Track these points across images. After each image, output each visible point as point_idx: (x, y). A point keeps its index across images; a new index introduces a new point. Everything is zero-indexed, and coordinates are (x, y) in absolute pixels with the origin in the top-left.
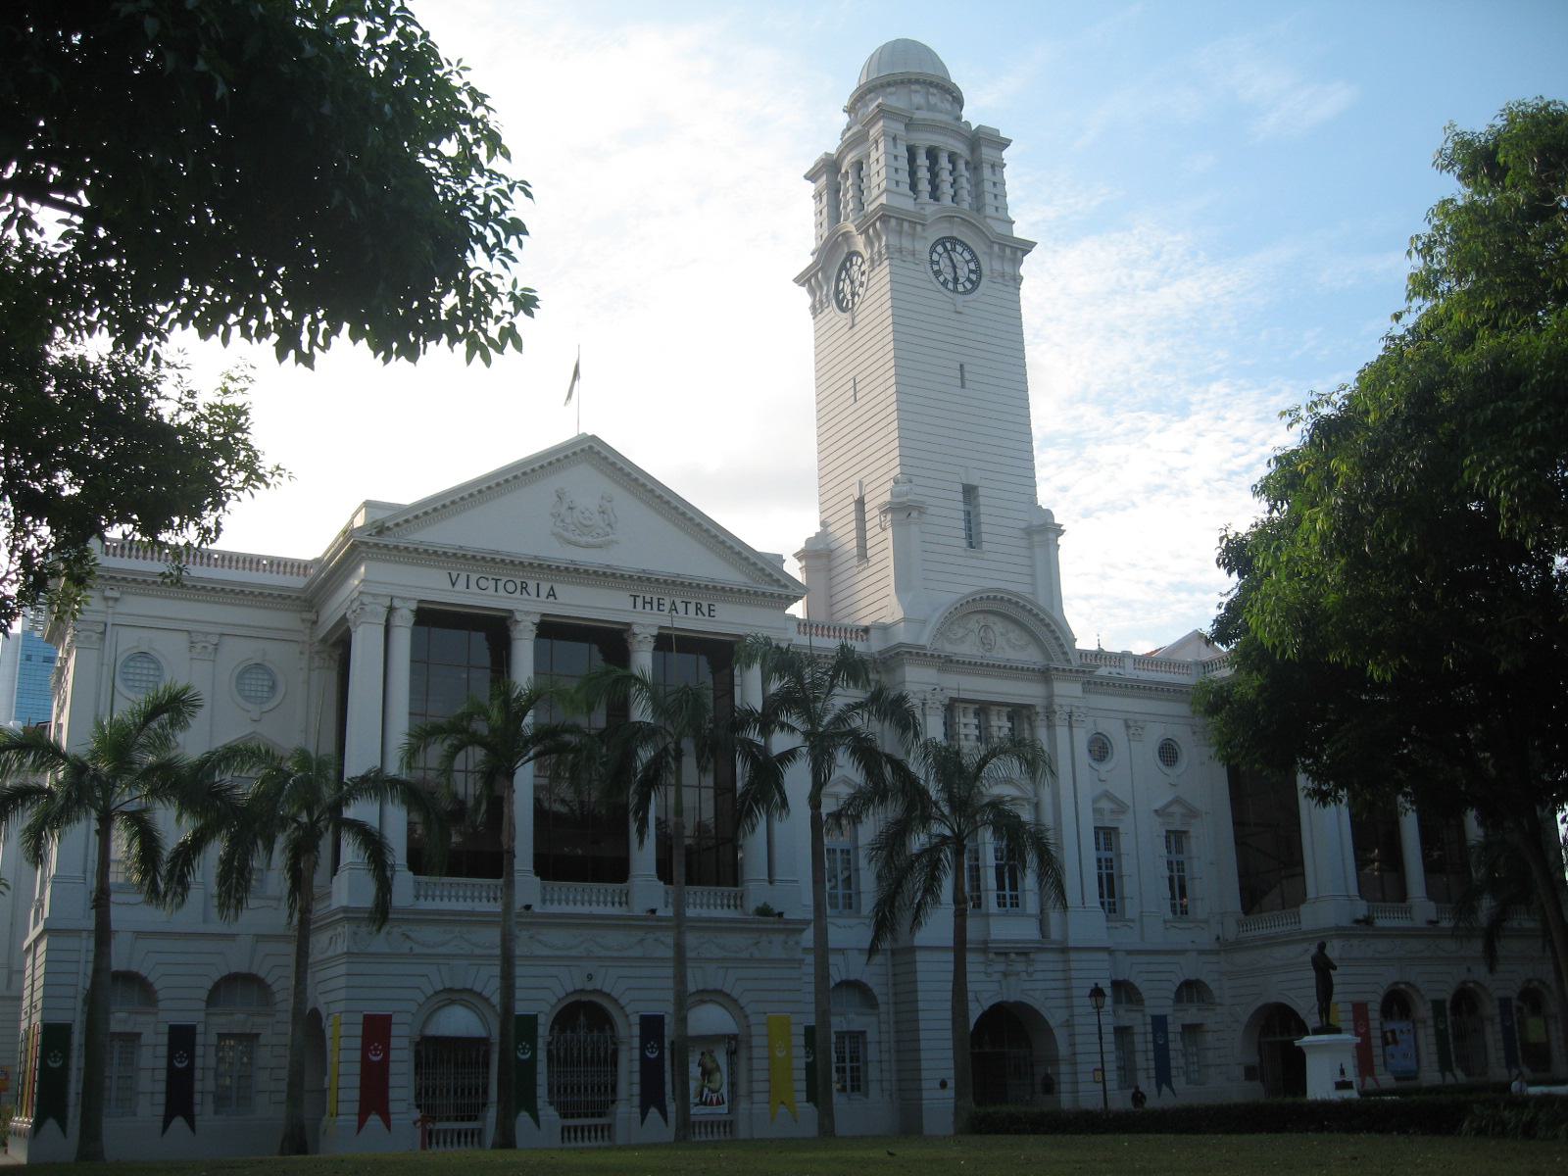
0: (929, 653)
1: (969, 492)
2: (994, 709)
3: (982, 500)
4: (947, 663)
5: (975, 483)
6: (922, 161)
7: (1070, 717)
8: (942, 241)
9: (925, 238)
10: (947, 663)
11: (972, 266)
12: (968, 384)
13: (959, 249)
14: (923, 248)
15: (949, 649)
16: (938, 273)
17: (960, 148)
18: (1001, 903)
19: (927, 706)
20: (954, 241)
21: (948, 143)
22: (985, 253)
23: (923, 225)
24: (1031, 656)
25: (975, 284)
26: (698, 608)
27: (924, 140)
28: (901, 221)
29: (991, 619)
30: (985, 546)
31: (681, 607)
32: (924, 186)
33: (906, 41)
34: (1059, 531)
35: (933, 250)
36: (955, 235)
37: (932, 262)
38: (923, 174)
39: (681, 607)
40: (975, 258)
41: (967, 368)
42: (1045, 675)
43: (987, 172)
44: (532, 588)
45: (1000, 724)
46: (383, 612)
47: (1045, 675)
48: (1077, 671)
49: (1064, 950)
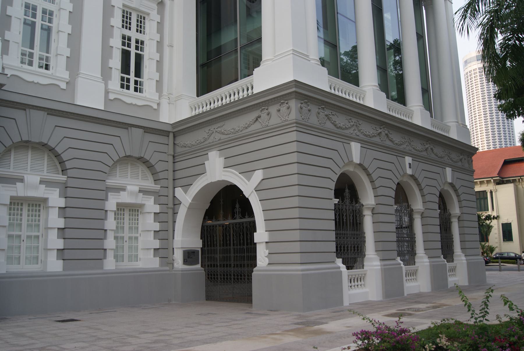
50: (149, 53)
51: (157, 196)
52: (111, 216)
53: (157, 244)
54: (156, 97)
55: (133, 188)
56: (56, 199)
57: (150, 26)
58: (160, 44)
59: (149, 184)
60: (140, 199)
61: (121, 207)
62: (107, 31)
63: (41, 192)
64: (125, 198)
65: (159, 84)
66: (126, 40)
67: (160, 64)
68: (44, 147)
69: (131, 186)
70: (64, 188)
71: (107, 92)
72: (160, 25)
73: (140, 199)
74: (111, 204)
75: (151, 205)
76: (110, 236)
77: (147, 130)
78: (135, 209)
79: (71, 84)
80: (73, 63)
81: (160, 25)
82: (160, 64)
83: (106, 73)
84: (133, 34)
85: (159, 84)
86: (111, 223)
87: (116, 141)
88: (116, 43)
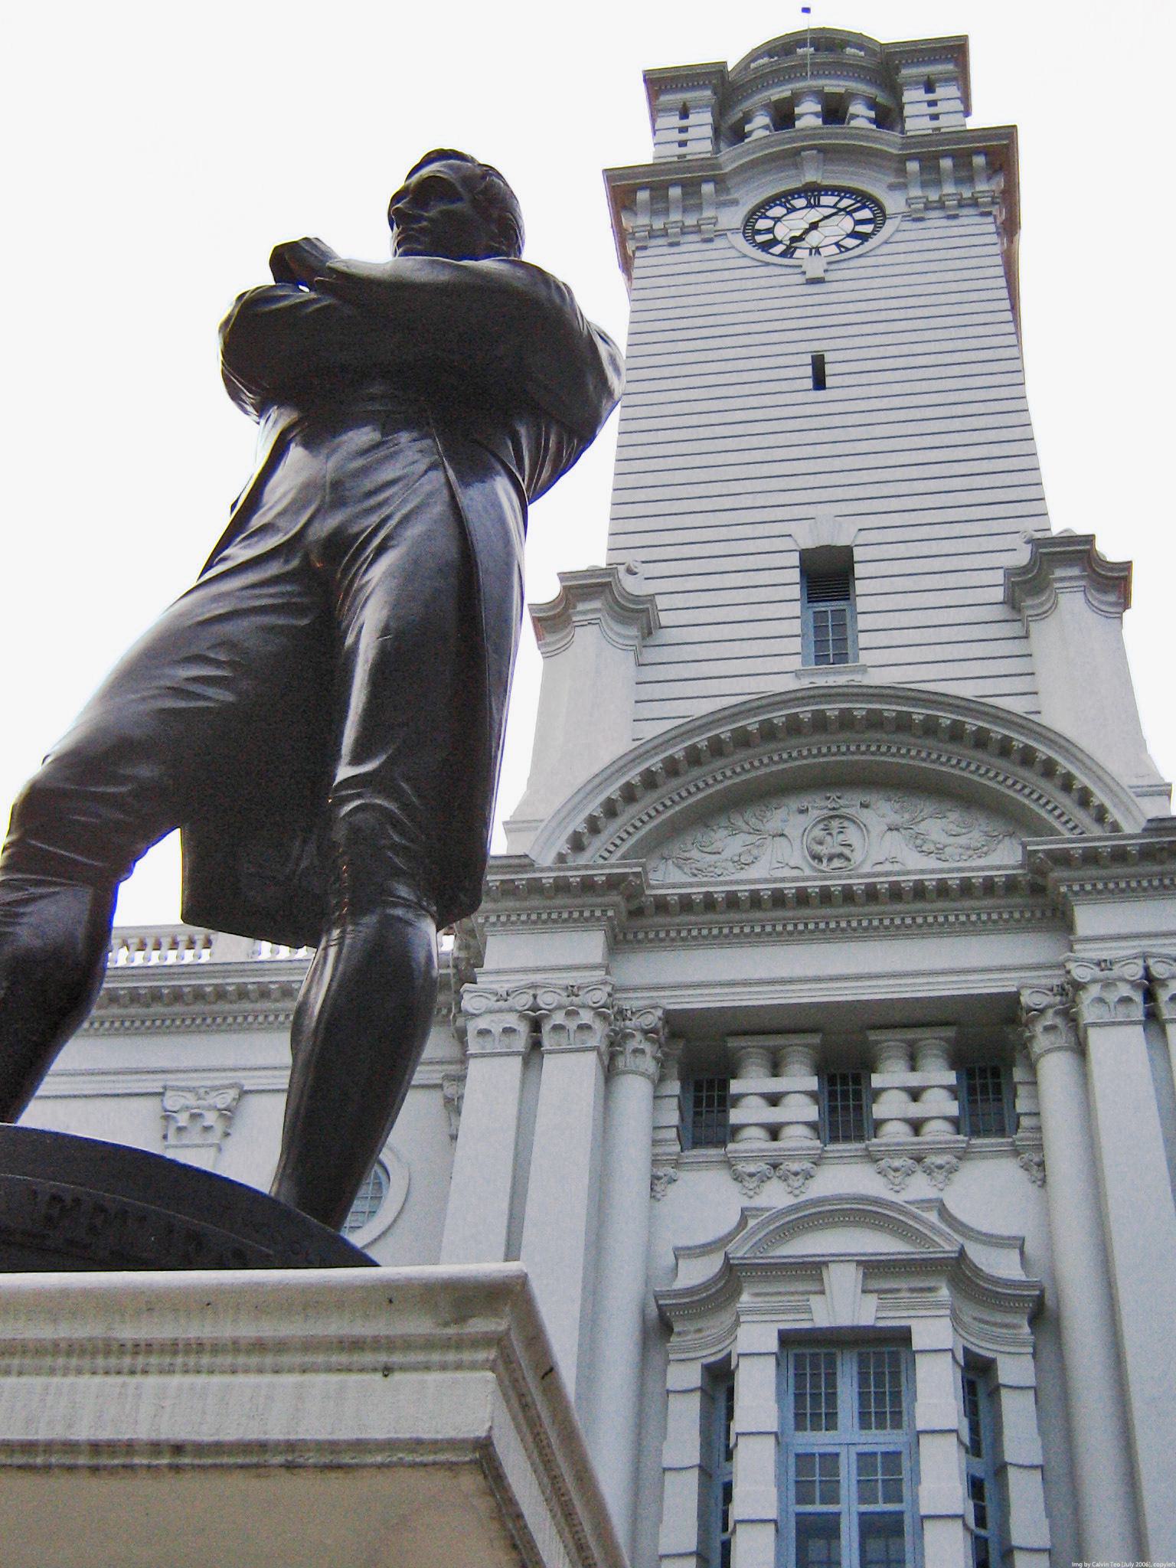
0: (548, 878)
3: (859, 570)
5: (842, 541)
7: (1150, 996)
8: (783, 198)
9: (735, 202)
10: (637, 917)
11: (866, 214)
12: (829, 382)
13: (827, 200)
14: (732, 218)
16: (765, 247)
19: (546, 1028)
22: (892, 187)
23: (720, 181)
24: (1004, 857)
28: (659, 190)
29: (850, 802)
30: (865, 658)
35: (759, 210)
36: (811, 176)
37: (759, 232)
40: (865, 199)
41: (828, 357)
42: (1037, 900)
45: (914, 1080)
48: (1148, 854)
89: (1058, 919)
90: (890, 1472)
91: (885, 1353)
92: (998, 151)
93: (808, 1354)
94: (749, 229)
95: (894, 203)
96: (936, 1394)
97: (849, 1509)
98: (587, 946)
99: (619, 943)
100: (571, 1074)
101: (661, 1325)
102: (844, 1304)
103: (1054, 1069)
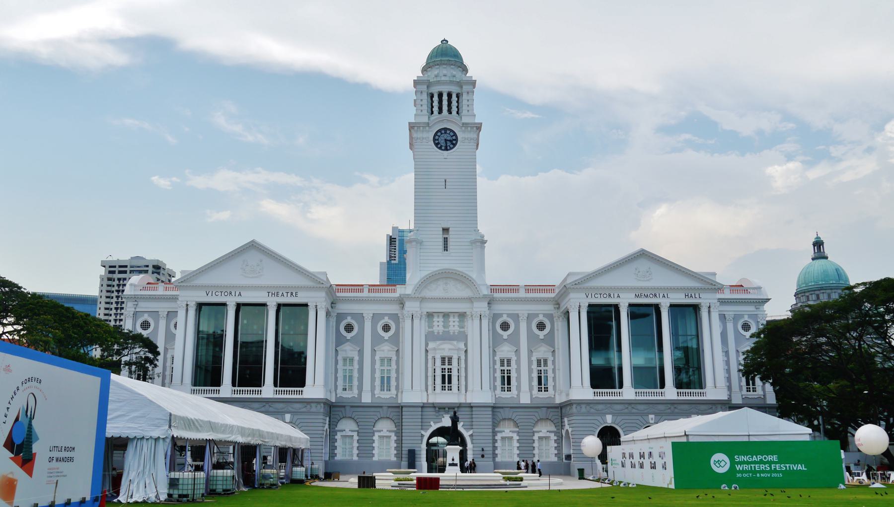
1: (446, 230)
2: (451, 315)
4: (423, 300)
6: (436, 99)
10: (423, 300)
15: (423, 294)
16: (436, 145)
17: (454, 90)
18: (443, 388)
20: (446, 129)
21: (445, 89)
24: (466, 293)
25: (455, 145)
26: (292, 294)
27: (435, 90)
31: (285, 294)
32: (436, 109)
33: (433, 52)
34: (485, 242)
35: (436, 134)
38: (436, 104)
39: (285, 294)
40: (455, 134)
42: (470, 300)
43: (465, 97)
44: (233, 294)
46: (184, 306)
47: (470, 300)
49: (472, 407)
50: (550, 375)
51: (556, 433)
52: (536, 442)
53: (556, 452)
54: (553, 392)
55: (544, 431)
56: (516, 437)
57: (550, 363)
58: (554, 371)
59: (553, 428)
60: (548, 434)
61: (540, 438)
62: (530, 371)
63: (511, 435)
64: (541, 435)
65: (554, 387)
66: (540, 372)
67: (554, 379)
68: (510, 419)
69: (544, 429)
70: (518, 433)
71: (531, 395)
72: (554, 362)
73: (548, 434)
74: (536, 437)
75: (553, 437)
76: (536, 449)
77: (548, 408)
78: (547, 438)
79: (518, 395)
80: (519, 388)
81: (554, 362)
82: (554, 379)
83: (531, 388)
84: (542, 368)
85: (554, 387)
86: (536, 445)
87: (536, 414)
88: (535, 375)
89: (472, 302)
90: (450, 370)
91: (450, 359)
92: (479, 127)
93: (443, 359)
94: (434, 140)
95: (460, 136)
96: (455, 362)
97: (447, 374)
98: (417, 304)
99: (421, 302)
100: (416, 321)
101: (427, 351)
102: (446, 354)
103: (470, 321)
